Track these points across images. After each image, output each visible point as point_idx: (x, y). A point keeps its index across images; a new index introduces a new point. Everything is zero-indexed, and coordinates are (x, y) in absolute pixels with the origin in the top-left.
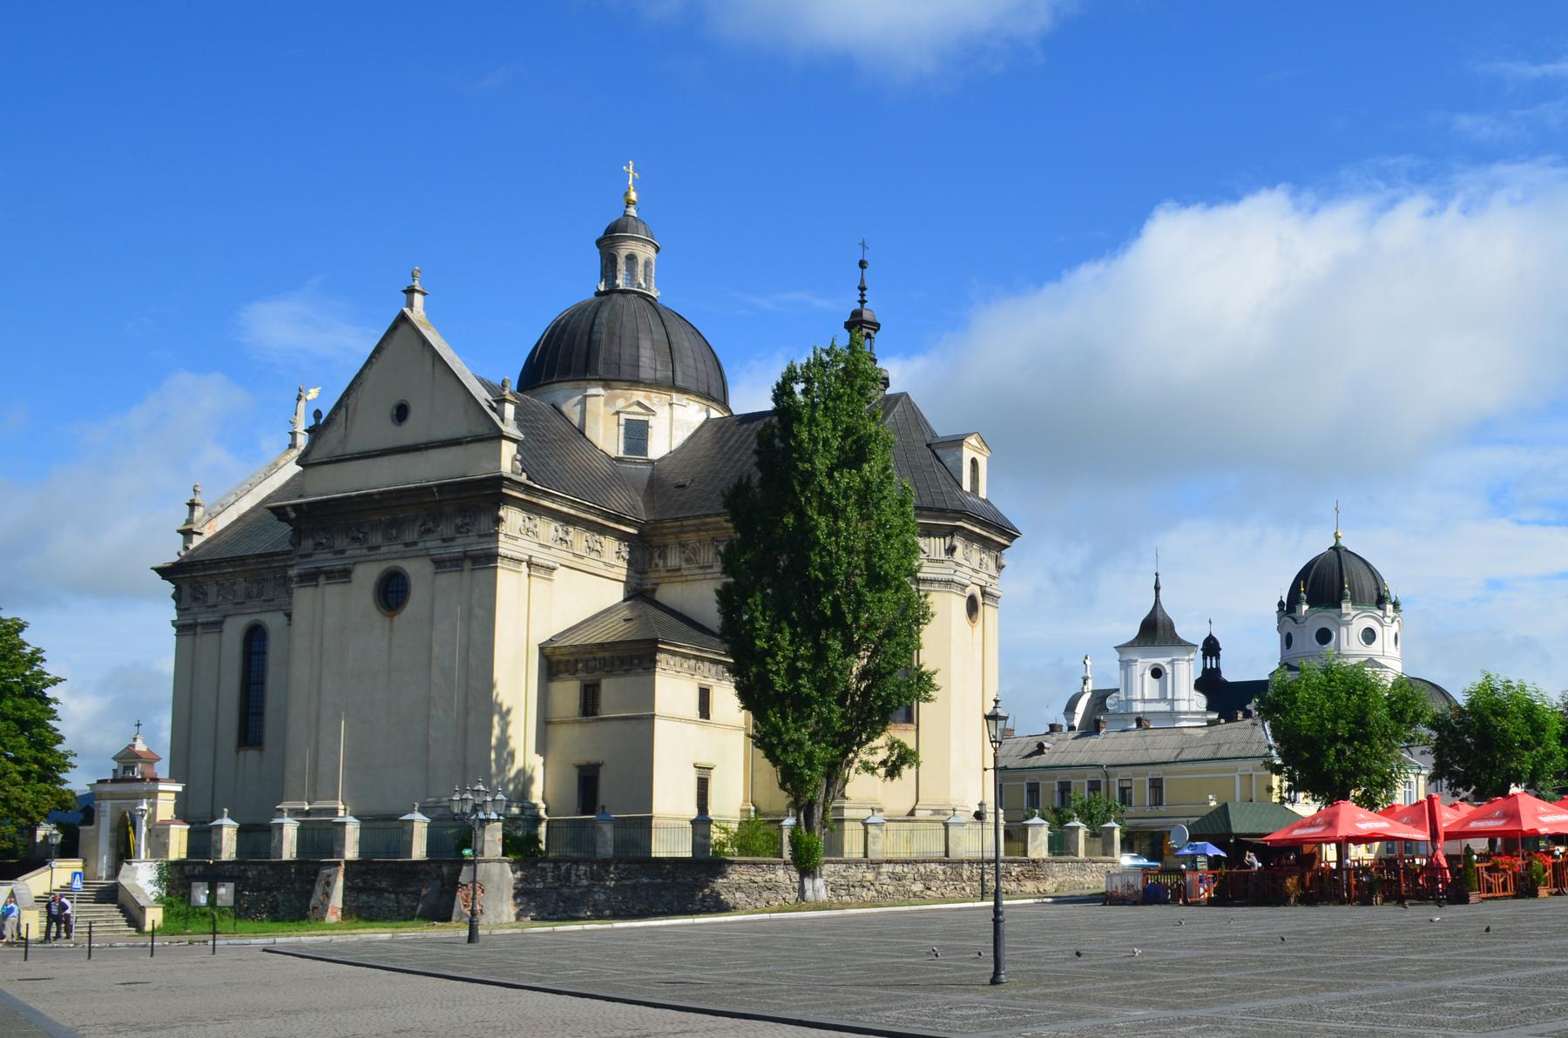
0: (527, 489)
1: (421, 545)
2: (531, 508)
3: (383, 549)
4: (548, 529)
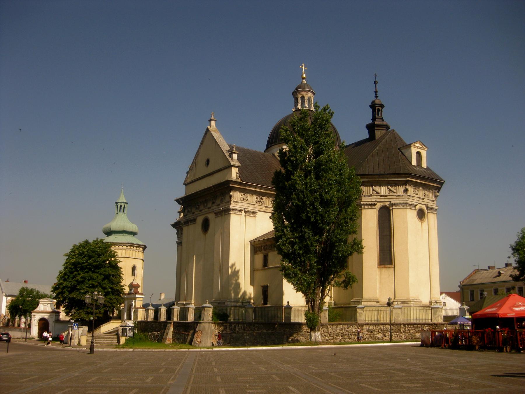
0: (240, 184)
1: (212, 208)
2: (244, 191)
3: (203, 211)
4: (252, 199)
